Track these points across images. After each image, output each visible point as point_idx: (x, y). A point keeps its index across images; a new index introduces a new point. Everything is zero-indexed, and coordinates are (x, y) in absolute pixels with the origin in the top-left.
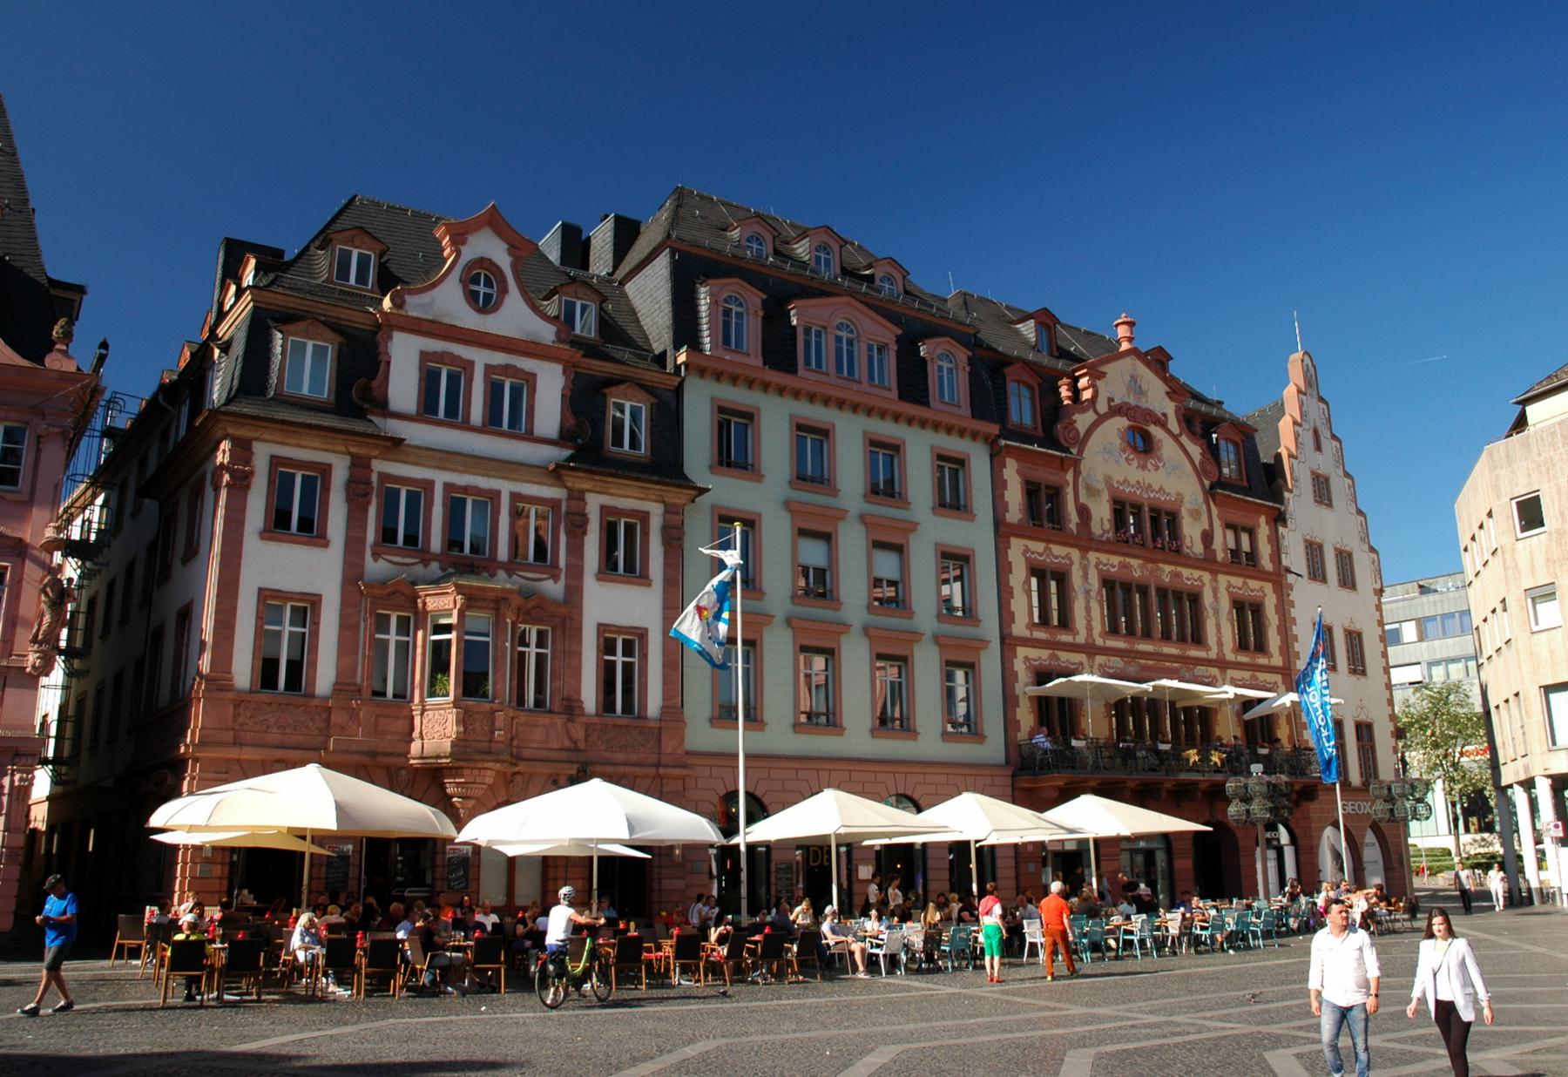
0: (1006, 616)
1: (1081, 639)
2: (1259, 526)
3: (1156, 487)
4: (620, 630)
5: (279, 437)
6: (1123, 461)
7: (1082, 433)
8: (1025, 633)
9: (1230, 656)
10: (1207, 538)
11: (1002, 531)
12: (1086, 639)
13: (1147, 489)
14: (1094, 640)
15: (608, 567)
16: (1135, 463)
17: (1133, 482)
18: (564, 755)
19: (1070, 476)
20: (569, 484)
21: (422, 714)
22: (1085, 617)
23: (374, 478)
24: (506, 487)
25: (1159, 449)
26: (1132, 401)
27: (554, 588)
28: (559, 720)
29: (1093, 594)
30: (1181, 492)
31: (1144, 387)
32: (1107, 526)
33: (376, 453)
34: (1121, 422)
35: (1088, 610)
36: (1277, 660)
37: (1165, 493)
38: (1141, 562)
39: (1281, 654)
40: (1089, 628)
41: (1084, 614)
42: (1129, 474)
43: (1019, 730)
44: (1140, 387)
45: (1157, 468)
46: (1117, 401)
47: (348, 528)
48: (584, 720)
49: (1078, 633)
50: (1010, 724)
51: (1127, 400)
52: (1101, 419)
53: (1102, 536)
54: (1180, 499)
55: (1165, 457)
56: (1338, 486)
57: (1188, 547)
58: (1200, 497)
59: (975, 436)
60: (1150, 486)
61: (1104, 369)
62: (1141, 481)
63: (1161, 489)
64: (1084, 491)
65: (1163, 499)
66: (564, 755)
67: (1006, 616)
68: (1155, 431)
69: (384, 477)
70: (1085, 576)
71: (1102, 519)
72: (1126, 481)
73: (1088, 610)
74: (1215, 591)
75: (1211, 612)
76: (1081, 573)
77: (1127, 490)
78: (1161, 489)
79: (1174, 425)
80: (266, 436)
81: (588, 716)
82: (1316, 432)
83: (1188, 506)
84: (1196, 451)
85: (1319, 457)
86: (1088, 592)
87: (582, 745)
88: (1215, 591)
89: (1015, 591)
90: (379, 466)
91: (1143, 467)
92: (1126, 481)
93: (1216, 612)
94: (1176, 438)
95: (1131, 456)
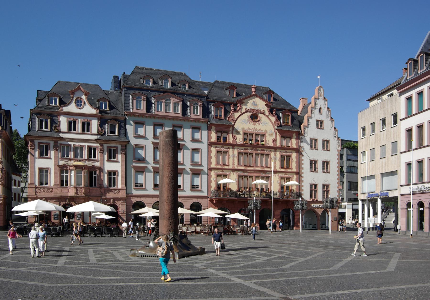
0: (209, 163)
1: (231, 167)
2: (293, 136)
3: (258, 129)
4: (112, 171)
5: (39, 139)
6: (248, 123)
7: (236, 117)
8: (214, 167)
9: (278, 169)
10: (274, 141)
11: (210, 144)
12: (232, 167)
13: (256, 130)
14: (235, 167)
15: (110, 157)
16: (252, 124)
17: (251, 128)
18: (99, 195)
19: (231, 129)
20: (99, 143)
21: (70, 189)
22: (233, 162)
23: (59, 145)
24: (86, 144)
25: (261, 119)
26: (253, 108)
27: (97, 164)
28: (98, 189)
29: (235, 157)
30: (266, 129)
31: (257, 104)
32: (241, 140)
33: (59, 140)
34: (249, 114)
35: (233, 160)
36: (295, 170)
37: (261, 130)
38: (251, 148)
39: (296, 168)
40: (233, 164)
41: (232, 161)
42: (251, 127)
43: (211, 188)
44: (256, 104)
45: (259, 124)
46: (248, 109)
47: (54, 155)
48: (104, 188)
49: (230, 166)
50: (209, 186)
51: (251, 108)
52: (242, 114)
53: (240, 142)
54: (266, 131)
55: (262, 121)
56: (327, 124)
57: (267, 143)
58: (273, 130)
59: (202, 122)
60: (256, 129)
61: (244, 101)
62: (254, 128)
63: (260, 130)
64: (235, 132)
65: (260, 132)
66: (99, 195)
67: (209, 163)
68: (260, 115)
69: (61, 144)
70: (234, 152)
71: (240, 138)
72: (249, 129)
73: (233, 160)
74: (275, 155)
75: (273, 159)
76: (232, 152)
77: (249, 131)
78: (260, 130)
79: (267, 113)
80: (36, 139)
81: (105, 187)
82: (320, 109)
83: (269, 133)
84: (273, 119)
85: (321, 116)
86: (234, 156)
87: (103, 193)
88: (275, 155)
89: (212, 157)
90: (60, 142)
91: (255, 125)
92: (249, 129)
93: (275, 159)
94: (267, 116)
95: (251, 122)
